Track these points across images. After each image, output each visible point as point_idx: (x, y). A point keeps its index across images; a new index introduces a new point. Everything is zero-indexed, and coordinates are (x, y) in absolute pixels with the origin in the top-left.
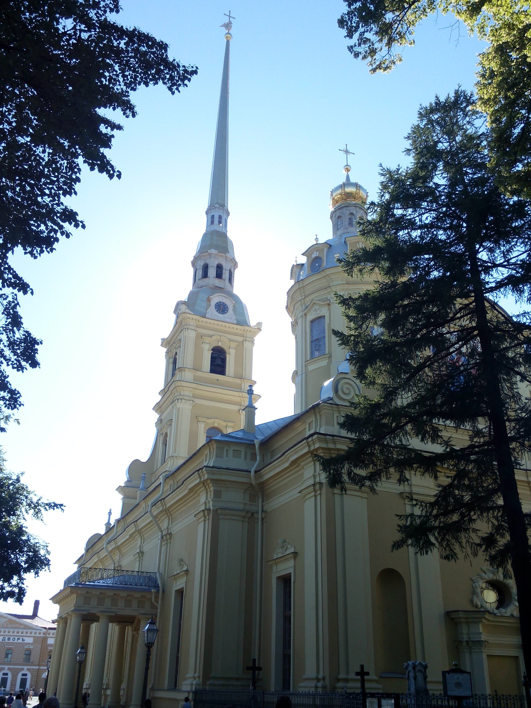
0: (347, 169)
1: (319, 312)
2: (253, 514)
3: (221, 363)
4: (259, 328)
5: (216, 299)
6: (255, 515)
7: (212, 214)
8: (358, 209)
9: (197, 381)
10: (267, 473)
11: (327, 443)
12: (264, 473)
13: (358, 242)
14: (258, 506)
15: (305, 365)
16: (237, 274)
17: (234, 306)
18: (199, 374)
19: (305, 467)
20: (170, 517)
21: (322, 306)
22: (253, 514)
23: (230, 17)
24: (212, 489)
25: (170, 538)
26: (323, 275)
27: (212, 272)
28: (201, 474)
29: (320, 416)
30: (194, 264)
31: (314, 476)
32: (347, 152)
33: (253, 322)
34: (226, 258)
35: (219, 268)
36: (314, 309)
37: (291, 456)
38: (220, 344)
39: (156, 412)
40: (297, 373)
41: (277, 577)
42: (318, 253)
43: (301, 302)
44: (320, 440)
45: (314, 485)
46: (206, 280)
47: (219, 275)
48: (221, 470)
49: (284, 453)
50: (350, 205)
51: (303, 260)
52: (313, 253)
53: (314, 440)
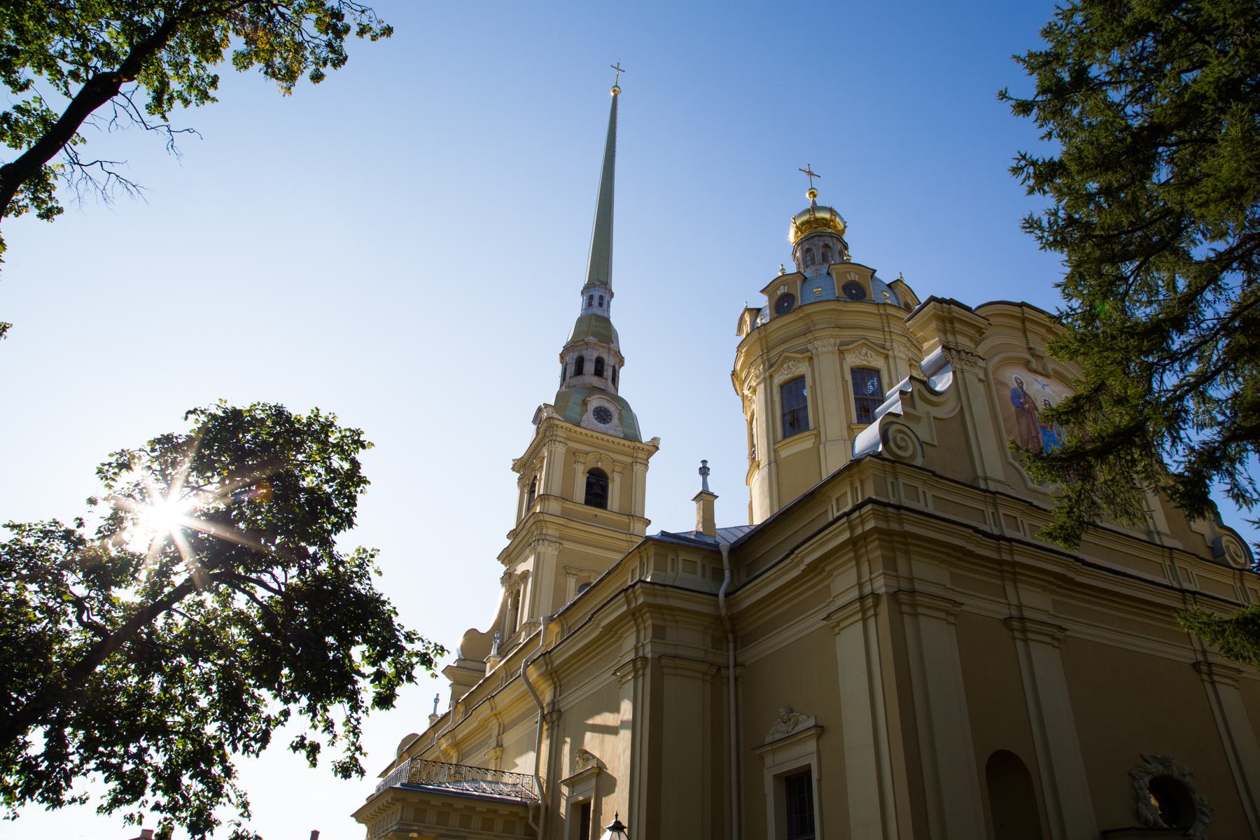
0: (813, 194)
2: (719, 670)
3: (600, 492)
4: (654, 446)
5: (595, 402)
6: (724, 672)
7: (591, 293)
8: (834, 239)
10: (748, 597)
11: (888, 521)
12: (741, 596)
13: (849, 273)
14: (728, 656)
15: (775, 450)
16: (623, 373)
18: (569, 505)
19: (835, 574)
20: (558, 684)
22: (719, 670)
24: (649, 622)
25: (559, 719)
26: (800, 316)
27: (589, 367)
28: (632, 596)
29: (862, 482)
30: (562, 356)
31: (860, 585)
32: (810, 173)
33: (646, 437)
35: (600, 363)
36: (785, 366)
37: (808, 554)
38: (599, 465)
39: (502, 563)
40: (759, 466)
41: (774, 776)
42: (786, 287)
44: (875, 515)
45: (862, 598)
46: (580, 379)
47: (599, 372)
48: (668, 588)
49: (792, 552)
52: (779, 288)
53: (864, 517)
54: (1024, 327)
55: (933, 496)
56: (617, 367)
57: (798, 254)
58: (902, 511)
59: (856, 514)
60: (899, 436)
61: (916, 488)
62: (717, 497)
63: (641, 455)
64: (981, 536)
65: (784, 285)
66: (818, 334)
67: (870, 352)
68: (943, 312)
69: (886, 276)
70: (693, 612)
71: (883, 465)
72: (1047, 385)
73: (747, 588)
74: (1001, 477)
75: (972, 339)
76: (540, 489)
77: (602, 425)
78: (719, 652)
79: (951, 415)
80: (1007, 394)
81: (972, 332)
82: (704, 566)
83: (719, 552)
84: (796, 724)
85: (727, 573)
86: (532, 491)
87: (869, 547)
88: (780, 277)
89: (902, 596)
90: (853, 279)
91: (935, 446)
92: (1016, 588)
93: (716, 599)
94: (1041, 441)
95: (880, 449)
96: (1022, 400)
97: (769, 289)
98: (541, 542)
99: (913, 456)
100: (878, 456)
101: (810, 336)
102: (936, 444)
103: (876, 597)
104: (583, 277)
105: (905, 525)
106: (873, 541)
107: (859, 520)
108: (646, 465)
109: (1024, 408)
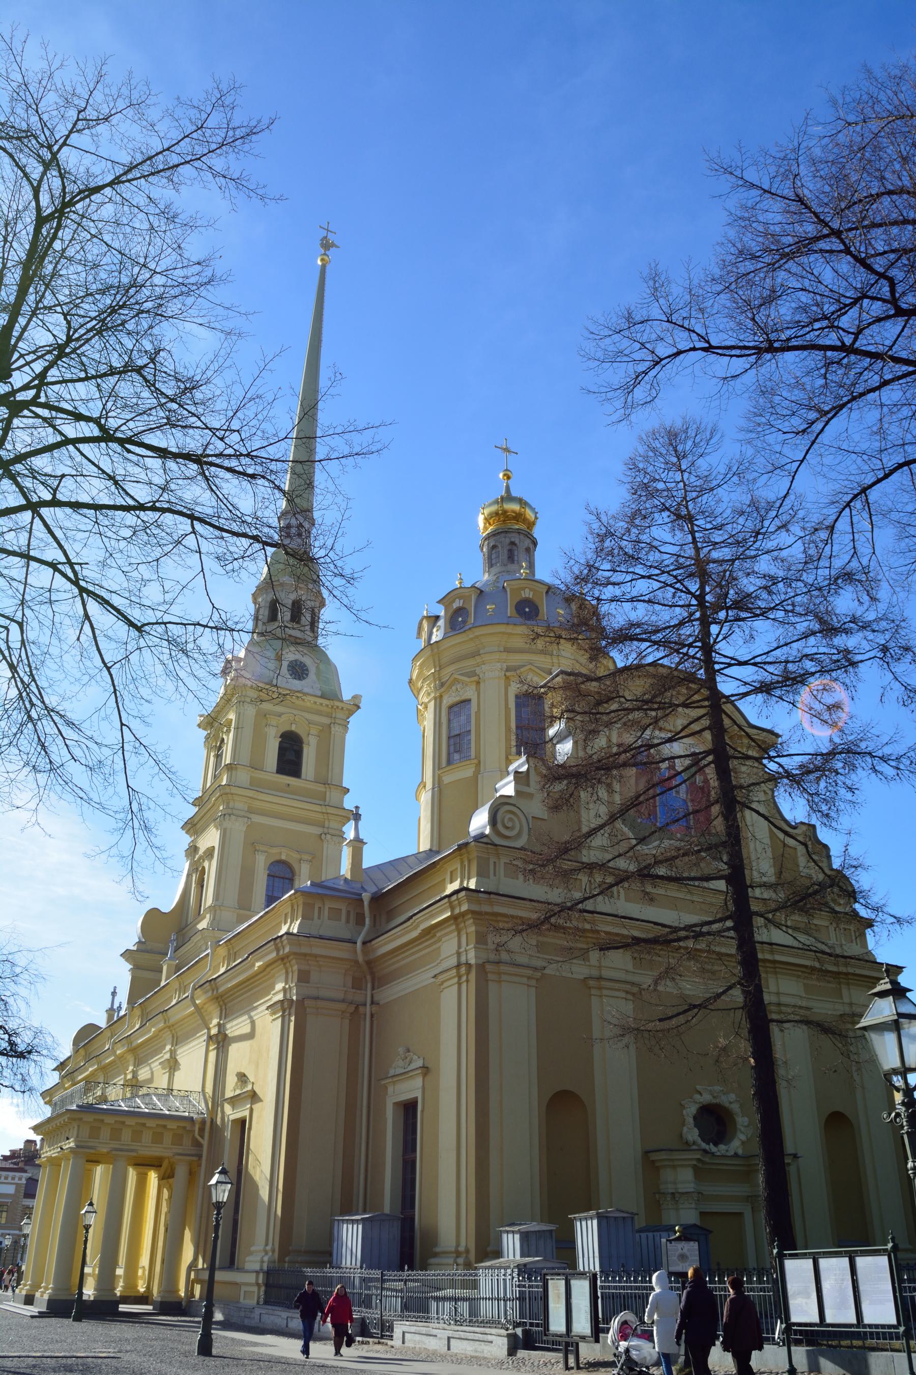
2: (357, 1008)
4: (355, 705)
6: (361, 1009)
8: (522, 536)
9: (255, 785)
22: (357, 1008)
24: (295, 968)
29: (469, 861)
31: (459, 954)
32: (507, 450)
33: (347, 696)
36: (454, 688)
38: (293, 728)
39: (187, 833)
42: (462, 601)
44: (469, 900)
45: (458, 966)
47: (296, 616)
52: (454, 601)
56: (316, 610)
57: (484, 550)
60: (509, 816)
63: (340, 715)
65: (460, 598)
70: (333, 958)
73: (386, 936)
76: (227, 759)
77: (297, 682)
82: (348, 913)
84: (410, 1062)
86: (218, 757)
90: (527, 596)
95: (487, 831)
97: (445, 600)
98: (227, 816)
101: (478, 659)
103: (468, 965)
108: (346, 727)
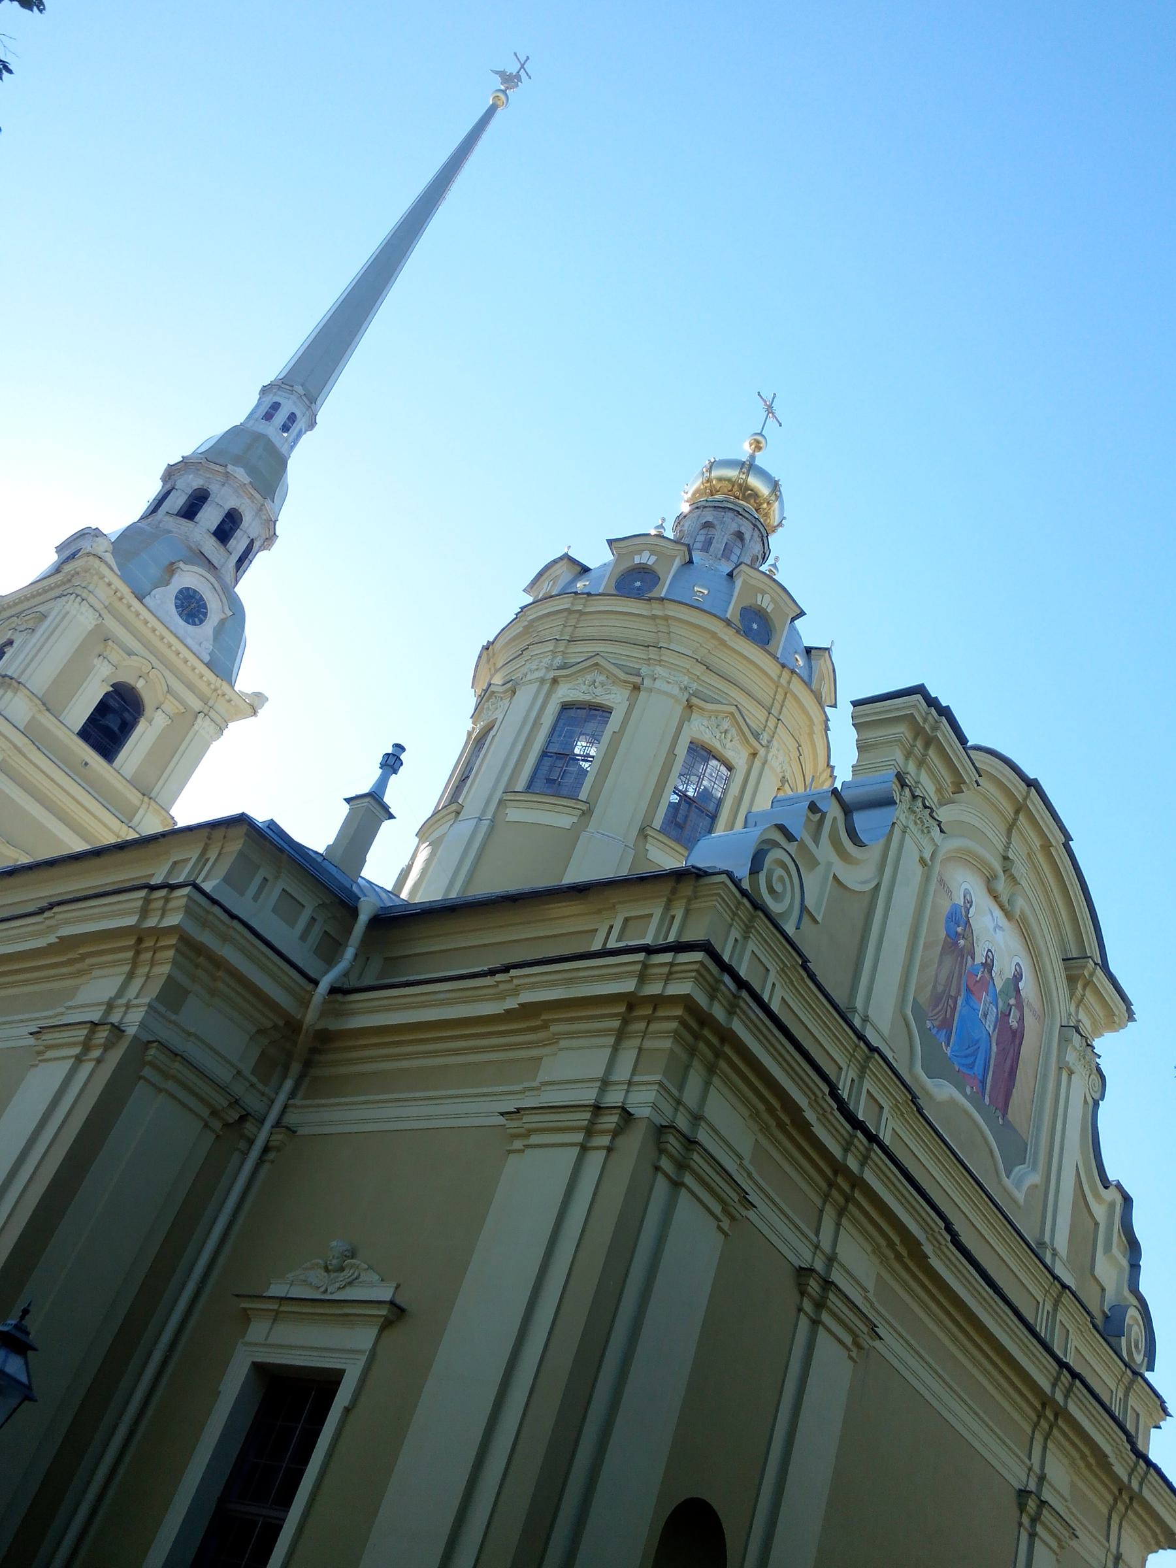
0: (758, 447)
1: (599, 691)
2: (243, 1119)
3: (116, 729)
4: (253, 705)
5: (190, 577)
6: (249, 1127)
7: (277, 399)
8: (756, 533)
9: (32, 733)
11: (712, 998)
13: (764, 593)
14: (272, 1101)
15: (501, 802)
16: (261, 561)
17: (222, 622)
18: (47, 721)
21: (616, 680)
22: (243, 1119)
23: (522, 66)
24: (166, 969)
27: (210, 517)
28: (160, 904)
30: (171, 473)
31: (605, 1084)
32: (770, 409)
34: (260, 510)
36: (589, 677)
37: (532, 986)
38: (140, 685)
41: (254, 1363)
42: (653, 558)
43: (556, 647)
44: (700, 976)
45: (598, 1109)
48: (235, 923)
49: (506, 969)
50: (746, 515)
51: (598, 556)
52: (640, 552)
54: (1015, 820)
55: (783, 998)
56: (257, 545)
58: (744, 994)
59: (667, 957)
60: (780, 872)
61: (768, 970)
62: (391, 817)
63: (221, 706)
64: (835, 1106)
65: (652, 553)
66: (667, 656)
67: (733, 731)
68: (925, 720)
69: (809, 632)
71: (739, 903)
72: (1001, 928)
74: (885, 1029)
75: (939, 790)
77: (181, 622)
78: (260, 1086)
79: (858, 888)
80: (945, 907)
81: (947, 778)
82: (313, 919)
83: (354, 912)
84: (350, 1283)
85: (350, 953)
87: (654, 1027)
88: (648, 535)
89: (672, 1139)
90: (764, 605)
91: (815, 921)
92: (838, 1225)
93: (310, 987)
94: (958, 1009)
96: (959, 929)
99: (786, 914)
100: (737, 883)
101: (653, 653)
102: (819, 919)
103: (627, 1116)
104: (273, 367)
105: (735, 1018)
106: (668, 1018)
107: (666, 970)
109: (956, 944)
